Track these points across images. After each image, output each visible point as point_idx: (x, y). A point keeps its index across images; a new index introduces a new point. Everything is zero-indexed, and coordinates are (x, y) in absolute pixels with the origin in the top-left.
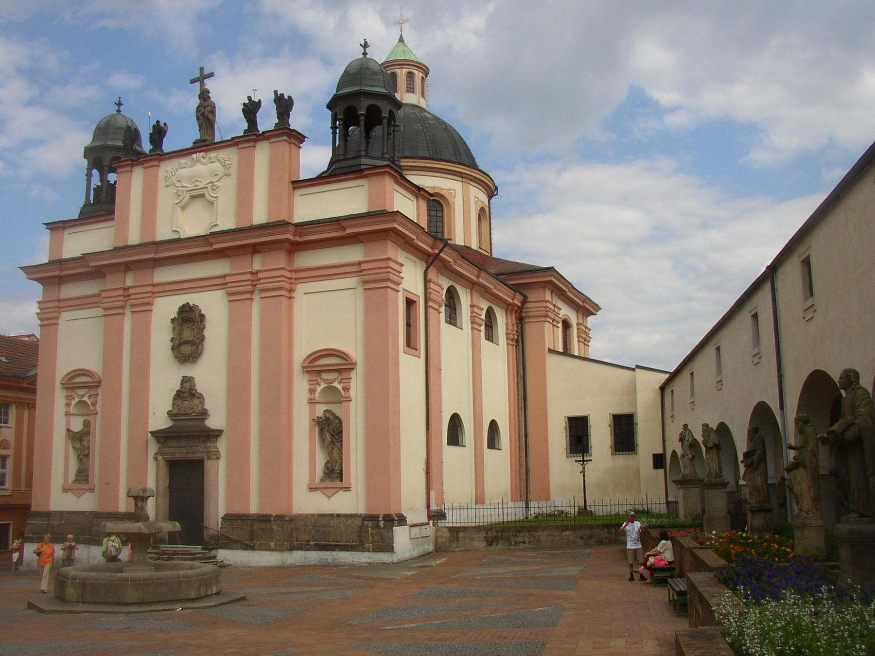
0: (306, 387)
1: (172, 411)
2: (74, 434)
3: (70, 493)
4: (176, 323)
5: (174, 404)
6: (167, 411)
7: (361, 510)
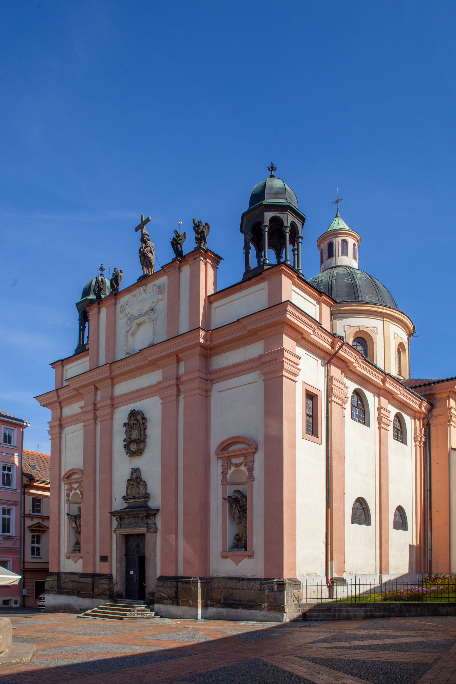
0: (220, 470)
2: (71, 517)
3: (70, 559)
6: (123, 496)
7: (260, 573)
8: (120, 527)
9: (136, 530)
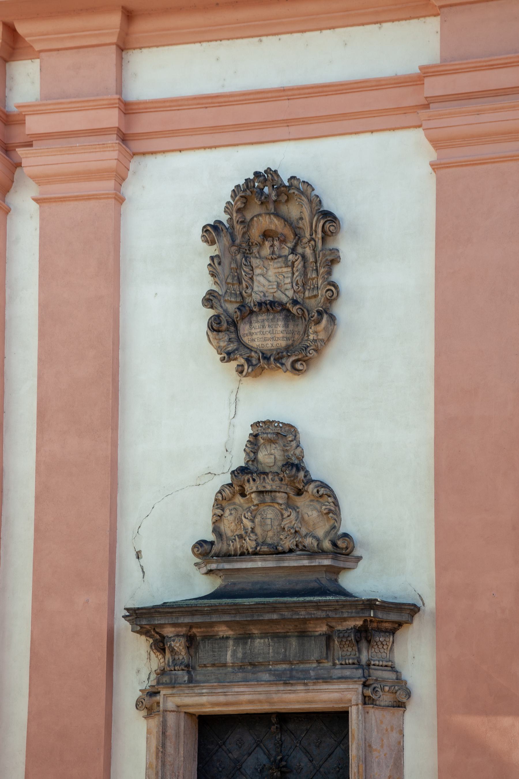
1: (212, 543)
4: (225, 240)
5: (218, 519)
8: (186, 678)
9: (294, 692)
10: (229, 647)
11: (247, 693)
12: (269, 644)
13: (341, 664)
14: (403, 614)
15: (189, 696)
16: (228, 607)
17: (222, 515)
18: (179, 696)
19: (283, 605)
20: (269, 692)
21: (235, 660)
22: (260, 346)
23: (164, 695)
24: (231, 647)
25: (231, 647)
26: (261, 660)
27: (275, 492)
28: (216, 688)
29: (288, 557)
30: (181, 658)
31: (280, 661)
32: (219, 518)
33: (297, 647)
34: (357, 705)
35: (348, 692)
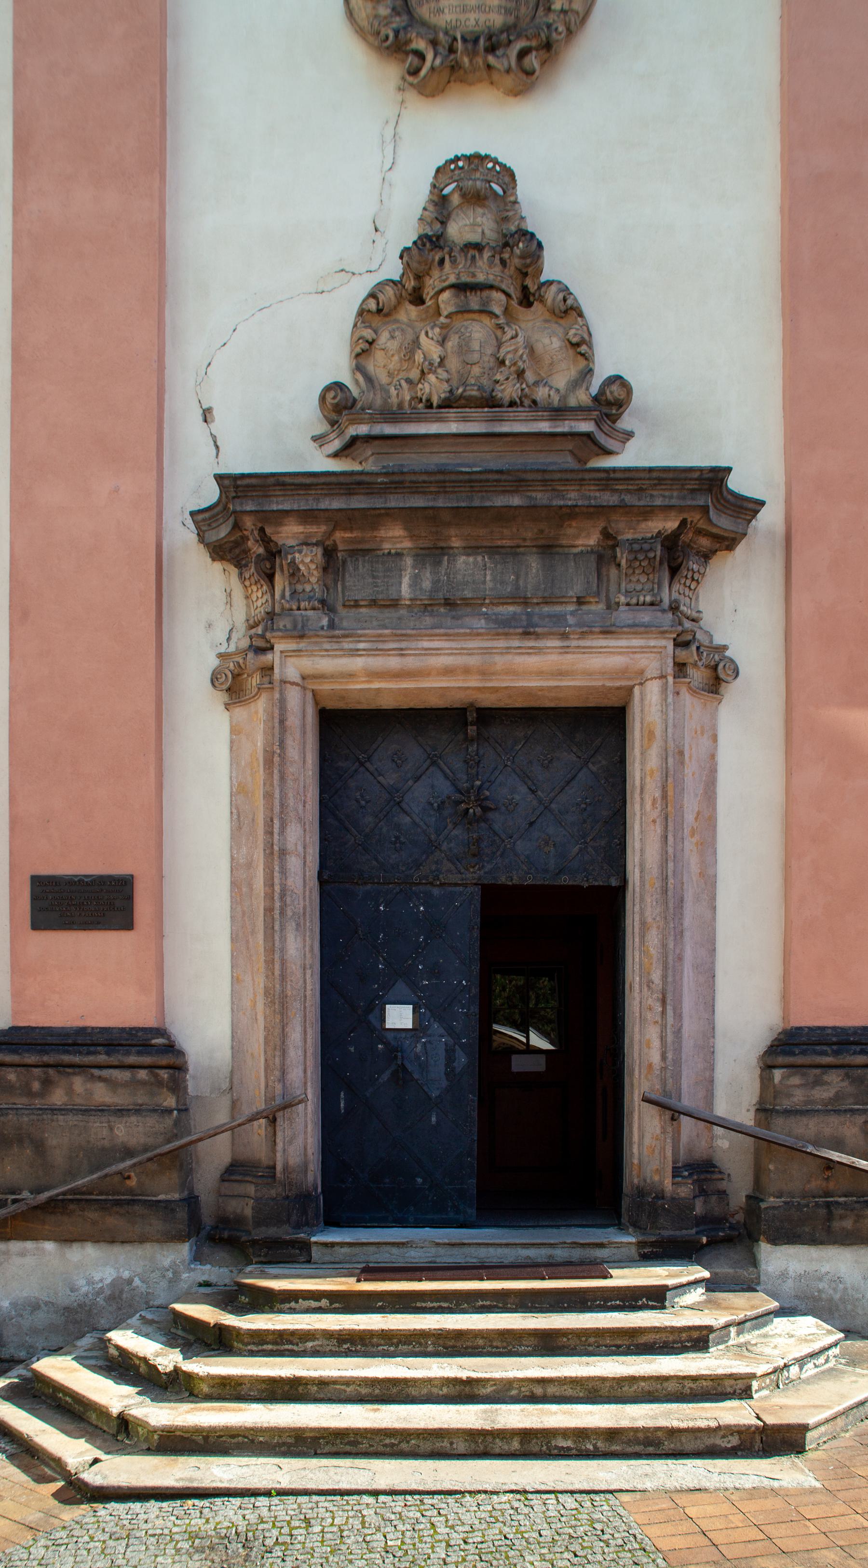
8: (325, 622)
9: (539, 651)
10: (405, 570)
11: (447, 652)
12: (485, 565)
13: (628, 604)
14: (740, 521)
15: (328, 656)
16: (425, 478)
17: (374, 341)
18: (311, 654)
19: (539, 476)
20: (490, 651)
21: (418, 593)
22: (454, 23)
23: (281, 652)
24: (409, 570)
25: (409, 570)
26: (468, 594)
27: (491, 287)
28: (385, 641)
29: (511, 414)
30: (308, 588)
31: (508, 597)
32: (367, 346)
33: (540, 572)
34: (663, 677)
35: (643, 655)
